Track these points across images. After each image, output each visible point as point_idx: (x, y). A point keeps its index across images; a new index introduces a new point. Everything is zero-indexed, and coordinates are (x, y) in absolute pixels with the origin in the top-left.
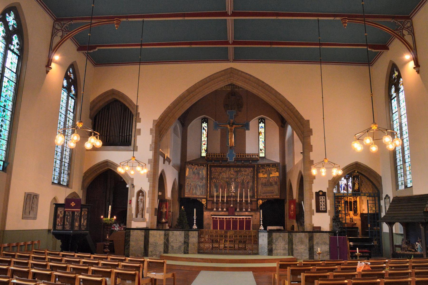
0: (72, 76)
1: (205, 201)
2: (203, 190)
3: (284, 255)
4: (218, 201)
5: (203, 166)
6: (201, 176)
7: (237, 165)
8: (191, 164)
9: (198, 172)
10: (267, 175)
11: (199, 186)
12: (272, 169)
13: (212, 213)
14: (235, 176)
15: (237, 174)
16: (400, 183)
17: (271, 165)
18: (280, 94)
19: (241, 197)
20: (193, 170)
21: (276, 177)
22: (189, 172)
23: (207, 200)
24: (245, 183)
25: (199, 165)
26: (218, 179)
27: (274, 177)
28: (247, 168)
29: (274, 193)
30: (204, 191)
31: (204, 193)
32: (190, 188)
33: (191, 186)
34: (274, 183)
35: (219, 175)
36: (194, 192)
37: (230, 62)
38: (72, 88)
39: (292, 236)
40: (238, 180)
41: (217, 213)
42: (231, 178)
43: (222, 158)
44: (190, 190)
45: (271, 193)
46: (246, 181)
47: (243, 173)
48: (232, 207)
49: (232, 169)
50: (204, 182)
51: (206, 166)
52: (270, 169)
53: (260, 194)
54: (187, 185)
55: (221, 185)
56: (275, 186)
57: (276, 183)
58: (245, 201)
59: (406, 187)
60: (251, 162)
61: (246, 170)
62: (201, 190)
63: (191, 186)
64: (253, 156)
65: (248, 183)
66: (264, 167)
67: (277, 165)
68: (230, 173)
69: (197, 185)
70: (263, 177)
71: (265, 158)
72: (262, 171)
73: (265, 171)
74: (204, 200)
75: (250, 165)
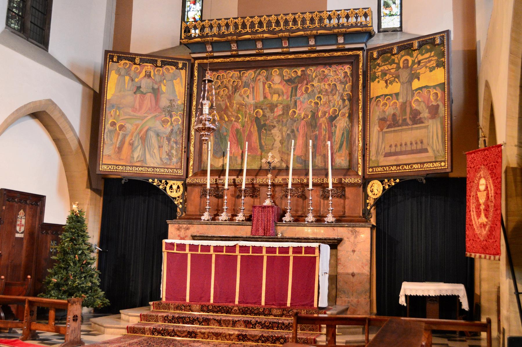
1: (178, 187)
2: (172, 148)
5: (176, 65)
6: (164, 102)
7: (292, 56)
9: (156, 87)
10: (402, 83)
11: (158, 135)
12: (420, 57)
14: (285, 97)
15: (295, 89)
17: (416, 45)
20: (132, 80)
21: (434, 87)
23: (185, 186)
24: (323, 121)
25: (159, 64)
27: (426, 87)
28: (330, 65)
29: (426, 151)
30: (174, 152)
31: (174, 160)
32: (123, 142)
33: (124, 137)
34: (425, 114)
35: (230, 97)
36: (136, 155)
40: (297, 112)
41: (211, 230)
42: (272, 107)
43: (240, 34)
44: (120, 149)
45: (412, 152)
46: (325, 113)
47: (315, 83)
49: (275, 72)
50: (177, 120)
51: (184, 65)
52: (413, 62)
53: (373, 158)
54: (110, 131)
55: (237, 131)
56: (431, 121)
57: (434, 111)
58: (314, 185)
61: (325, 76)
62: (166, 148)
63: (124, 137)
64: (347, 17)
65: (333, 119)
66: (389, 55)
67: (438, 41)
68: (270, 87)
69: (147, 131)
70: (386, 95)
71: (401, 30)
72: (384, 74)
73: (393, 71)
74: (176, 184)
75: (339, 54)
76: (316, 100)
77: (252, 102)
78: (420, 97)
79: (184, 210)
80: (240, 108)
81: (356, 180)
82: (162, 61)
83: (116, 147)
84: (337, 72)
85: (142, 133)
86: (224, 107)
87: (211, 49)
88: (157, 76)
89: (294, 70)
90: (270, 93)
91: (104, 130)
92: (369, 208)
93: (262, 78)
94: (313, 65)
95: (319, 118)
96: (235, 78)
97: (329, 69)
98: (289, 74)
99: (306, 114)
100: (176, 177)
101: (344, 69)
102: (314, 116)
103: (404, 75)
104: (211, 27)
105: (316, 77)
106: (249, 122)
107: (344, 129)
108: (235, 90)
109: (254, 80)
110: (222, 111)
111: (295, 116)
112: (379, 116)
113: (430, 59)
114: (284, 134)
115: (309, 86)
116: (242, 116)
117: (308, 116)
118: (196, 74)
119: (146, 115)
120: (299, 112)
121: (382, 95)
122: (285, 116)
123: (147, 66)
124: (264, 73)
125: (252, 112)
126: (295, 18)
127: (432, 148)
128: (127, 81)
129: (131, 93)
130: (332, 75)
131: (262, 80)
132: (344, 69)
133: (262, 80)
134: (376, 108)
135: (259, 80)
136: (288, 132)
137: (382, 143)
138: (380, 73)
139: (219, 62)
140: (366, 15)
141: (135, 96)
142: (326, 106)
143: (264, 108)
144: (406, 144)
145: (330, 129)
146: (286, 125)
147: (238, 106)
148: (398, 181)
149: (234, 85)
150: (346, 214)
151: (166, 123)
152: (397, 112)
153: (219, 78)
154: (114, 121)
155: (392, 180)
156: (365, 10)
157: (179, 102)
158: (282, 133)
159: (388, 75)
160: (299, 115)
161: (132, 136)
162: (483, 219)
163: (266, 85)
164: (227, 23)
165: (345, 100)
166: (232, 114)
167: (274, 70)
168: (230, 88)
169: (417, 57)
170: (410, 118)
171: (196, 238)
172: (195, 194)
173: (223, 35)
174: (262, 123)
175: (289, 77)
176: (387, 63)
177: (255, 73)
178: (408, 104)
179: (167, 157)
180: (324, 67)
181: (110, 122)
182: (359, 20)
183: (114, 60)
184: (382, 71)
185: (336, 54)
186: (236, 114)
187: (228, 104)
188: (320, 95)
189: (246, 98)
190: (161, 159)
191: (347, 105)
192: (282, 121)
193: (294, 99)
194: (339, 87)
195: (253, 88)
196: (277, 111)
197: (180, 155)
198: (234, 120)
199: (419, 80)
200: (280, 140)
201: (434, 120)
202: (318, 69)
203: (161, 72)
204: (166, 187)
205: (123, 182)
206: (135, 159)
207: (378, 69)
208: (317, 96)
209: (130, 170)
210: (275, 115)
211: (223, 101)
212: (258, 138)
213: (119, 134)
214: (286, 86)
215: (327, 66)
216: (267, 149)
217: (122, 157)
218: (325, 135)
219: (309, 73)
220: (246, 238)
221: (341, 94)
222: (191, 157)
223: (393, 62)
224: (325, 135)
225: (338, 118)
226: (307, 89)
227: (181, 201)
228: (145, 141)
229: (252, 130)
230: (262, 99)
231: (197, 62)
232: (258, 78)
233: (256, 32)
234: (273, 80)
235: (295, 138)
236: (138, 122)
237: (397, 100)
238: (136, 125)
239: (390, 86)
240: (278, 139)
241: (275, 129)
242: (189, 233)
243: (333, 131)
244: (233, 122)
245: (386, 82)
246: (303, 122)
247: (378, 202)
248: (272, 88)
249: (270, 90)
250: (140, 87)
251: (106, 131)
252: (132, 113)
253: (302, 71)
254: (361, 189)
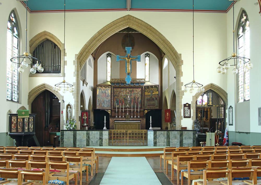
0: (14, 20)
3: (164, 146)
4: (118, 111)
5: (109, 87)
8: (100, 86)
10: (151, 93)
11: (106, 101)
13: (115, 119)
16: (240, 98)
17: (153, 87)
18: (162, 35)
19: (134, 108)
20: (101, 90)
26: (118, 96)
29: (155, 105)
32: (100, 103)
35: (119, 94)
37: (128, 10)
38: (15, 29)
39: (169, 133)
41: (118, 119)
43: (121, 82)
45: (153, 105)
48: (127, 115)
49: (127, 89)
51: (110, 87)
57: (156, 99)
59: (245, 100)
60: (140, 84)
65: (138, 98)
68: (126, 92)
79: (111, 115)
103: (151, 92)
104: (116, 80)
109: (124, 91)
124: (125, 89)
157: (110, 95)
162: (168, 118)
172: (113, 112)
194: (139, 93)
205: (101, 110)
230: (125, 94)
247: (146, 114)
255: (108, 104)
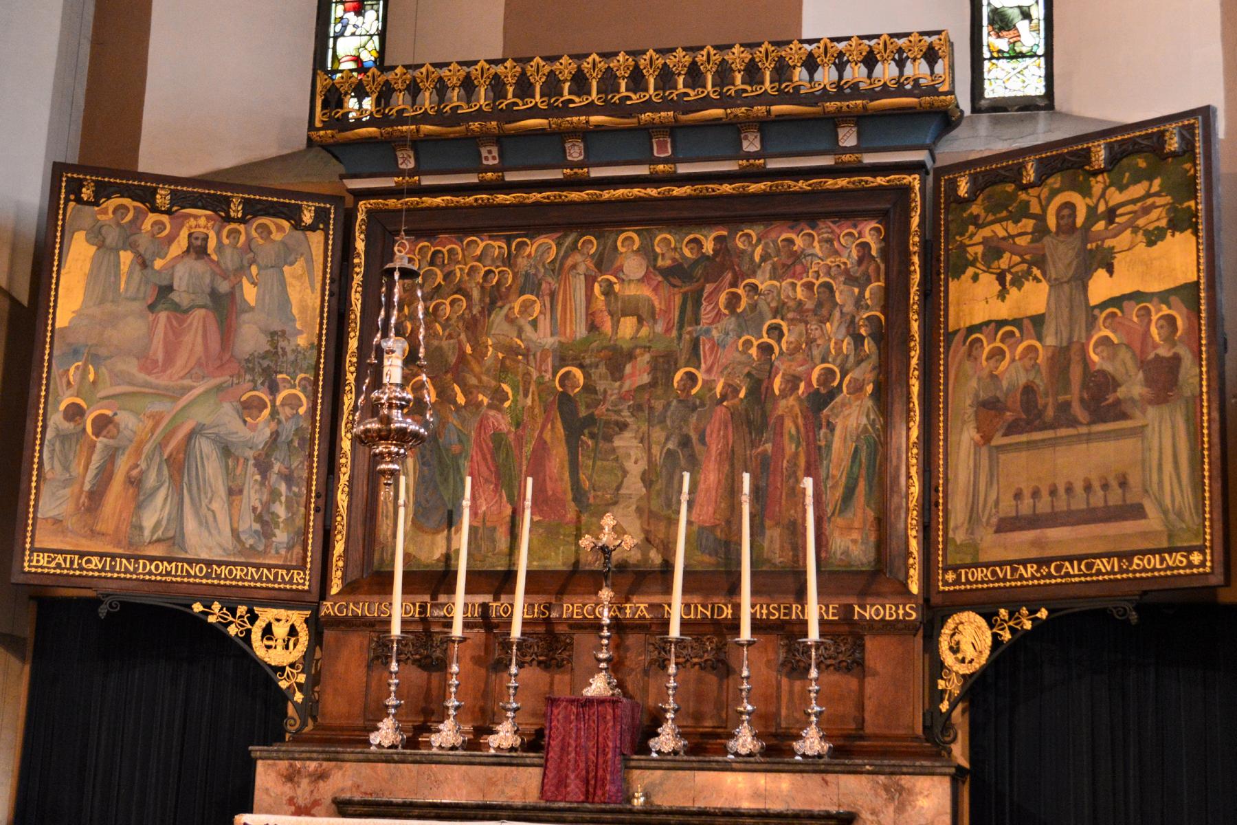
1: (293, 632)
2: (274, 495)
5: (293, 215)
6: (250, 339)
7: (686, 190)
9: (224, 287)
10: (1055, 284)
11: (226, 451)
12: (1115, 197)
14: (659, 328)
15: (693, 303)
17: (1100, 155)
20: (144, 264)
21: (1164, 297)
22: (93, 277)
23: (317, 626)
24: (788, 408)
25: (236, 210)
27: (1137, 296)
28: (812, 219)
29: (1137, 512)
30: (281, 510)
31: (281, 536)
32: (105, 475)
34: (1134, 387)
35: (473, 326)
36: (149, 520)
40: (700, 376)
42: (617, 359)
44: (96, 496)
46: (793, 382)
49: (628, 241)
50: (293, 402)
51: (321, 216)
52: (1092, 213)
53: (960, 537)
54: (63, 437)
55: (498, 438)
56: (1152, 412)
58: (757, 626)
60: (848, 138)
61: (797, 257)
64: (870, 61)
65: (821, 400)
66: (1010, 188)
67: (1174, 144)
68: (608, 291)
69: (190, 436)
70: (1001, 323)
72: (994, 250)
73: (1022, 241)
74: (284, 620)
75: (842, 182)
76: (766, 339)
77: (550, 341)
78: (1114, 331)
79: (310, 709)
80: (508, 362)
81: (901, 612)
82: (246, 203)
83: (81, 491)
84: (836, 244)
85: (173, 444)
86: (453, 360)
87: (411, 164)
88: (228, 252)
89: (691, 236)
90: (611, 314)
91: (43, 432)
92: (944, 707)
93: (582, 263)
94: (751, 220)
95: (775, 399)
96: (493, 260)
97: (810, 235)
98: (675, 249)
99: (730, 385)
100: (283, 595)
101: (860, 233)
102: (759, 389)
103: (1063, 255)
105: (764, 258)
106: (536, 411)
107: (858, 437)
108: (493, 302)
109: (558, 268)
110: (447, 372)
111: (694, 391)
112: (977, 395)
113: (1149, 201)
114: (656, 450)
115: (740, 291)
116: (515, 388)
117: (736, 391)
118: (360, 245)
119: (187, 382)
120: (706, 377)
121: (987, 323)
122: (659, 391)
123: (196, 217)
125: (548, 376)
126: (694, 63)
127: (1160, 504)
128: (124, 268)
129: (137, 306)
130: (820, 254)
131: (582, 269)
132: (860, 233)
133: (582, 269)
134: (968, 365)
135: (574, 267)
136: (670, 446)
137: (990, 483)
138: (980, 249)
139: (438, 208)
140: (931, 56)
141: (151, 317)
142: (800, 357)
143: (588, 361)
144: (1069, 489)
145: (811, 434)
146: (662, 421)
147: (500, 355)
148: (1043, 614)
149: (488, 285)
150: (869, 729)
151: (255, 412)
152: (1037, 381)
153: (439, 261)
154: (78, 401)
155: (1024, 611)
156: (928, 39)
157: (302, 341)
158: (650, 449)
159: (1007, 255)
160: (709, 386)
161: (138, 451)
163: (597, 286)
164: (468, 76)
165: (864, 338)
166: (480, 381)
167: (622, 236)
168: (476, 294)
169: (1103, 195)
170: (1082, 400)
171: (351, 809)
173: (455, 118)
174: (583, 412)
175: (674, 259)
176: (1004, 213)
177: (559, 245)
178: (1075, 358)
179: (257, 526)
180: (792, 228)
181: (62, 407)
182: (909, 70)
183: (85, 197)
184: (985, 242)
185: (830, 183)
186: (493, 383)
187: (468, 350)
188: (778, 321)
189: (528, 329)
190: (235, 533)
191: (868, 356)
192: (651, 408)
193: (689, 333)
194: (843, 294)
195: (553, 295)
196: (632, 375)
197: (299, 522)
198: (486, 401)
199: (1110, 271)
200: (644, 473)
201: (1165, 409)
202: (773, 235)
203: (243, 238)
204: (249, 632)
205: (103, 611)
206: (147, 533)
207: (973, 235)
208: (768, 323)
209: (127, 571)
210: (627, 385)
211: (450, 337)
212: (566, 465)
213: (93, 446)
214: (665, 290)
215: (803, 225)
216: (598, 501)
217: (100, 527)
218: (796, 454)
219: (740, 245)
220: (524, 808)
221: (849, 317)
222: (339, 527)
223: (1023, 212)
224: (796, 454)
225: (838, 399)
226: (734, 300)
227: (302, 678)
228: (180, 471)
229: (547, 436)
230: (581, 331)
231: (362, 205)
232: (570, 262)
233: (565, 110)
234: (621, 269)
235: (694, 465)
236: (157, 407)
237: (1040, 338)
238: (152, 416)
239: (1014, 291)
240: (635, 468)
241: (627, 434)
242: (328, 790)
243: (823, 443)
244: (484, 409)
245: (1001, 278)
246: (720, 412)
247: (976, 686)
248: (616, 295)
249: (608, 304)
250: (170, 288)
251: (50, 434)
252: (142, 376)
253: (718, 239)
254: (919, 641)
255: (253, 497)
